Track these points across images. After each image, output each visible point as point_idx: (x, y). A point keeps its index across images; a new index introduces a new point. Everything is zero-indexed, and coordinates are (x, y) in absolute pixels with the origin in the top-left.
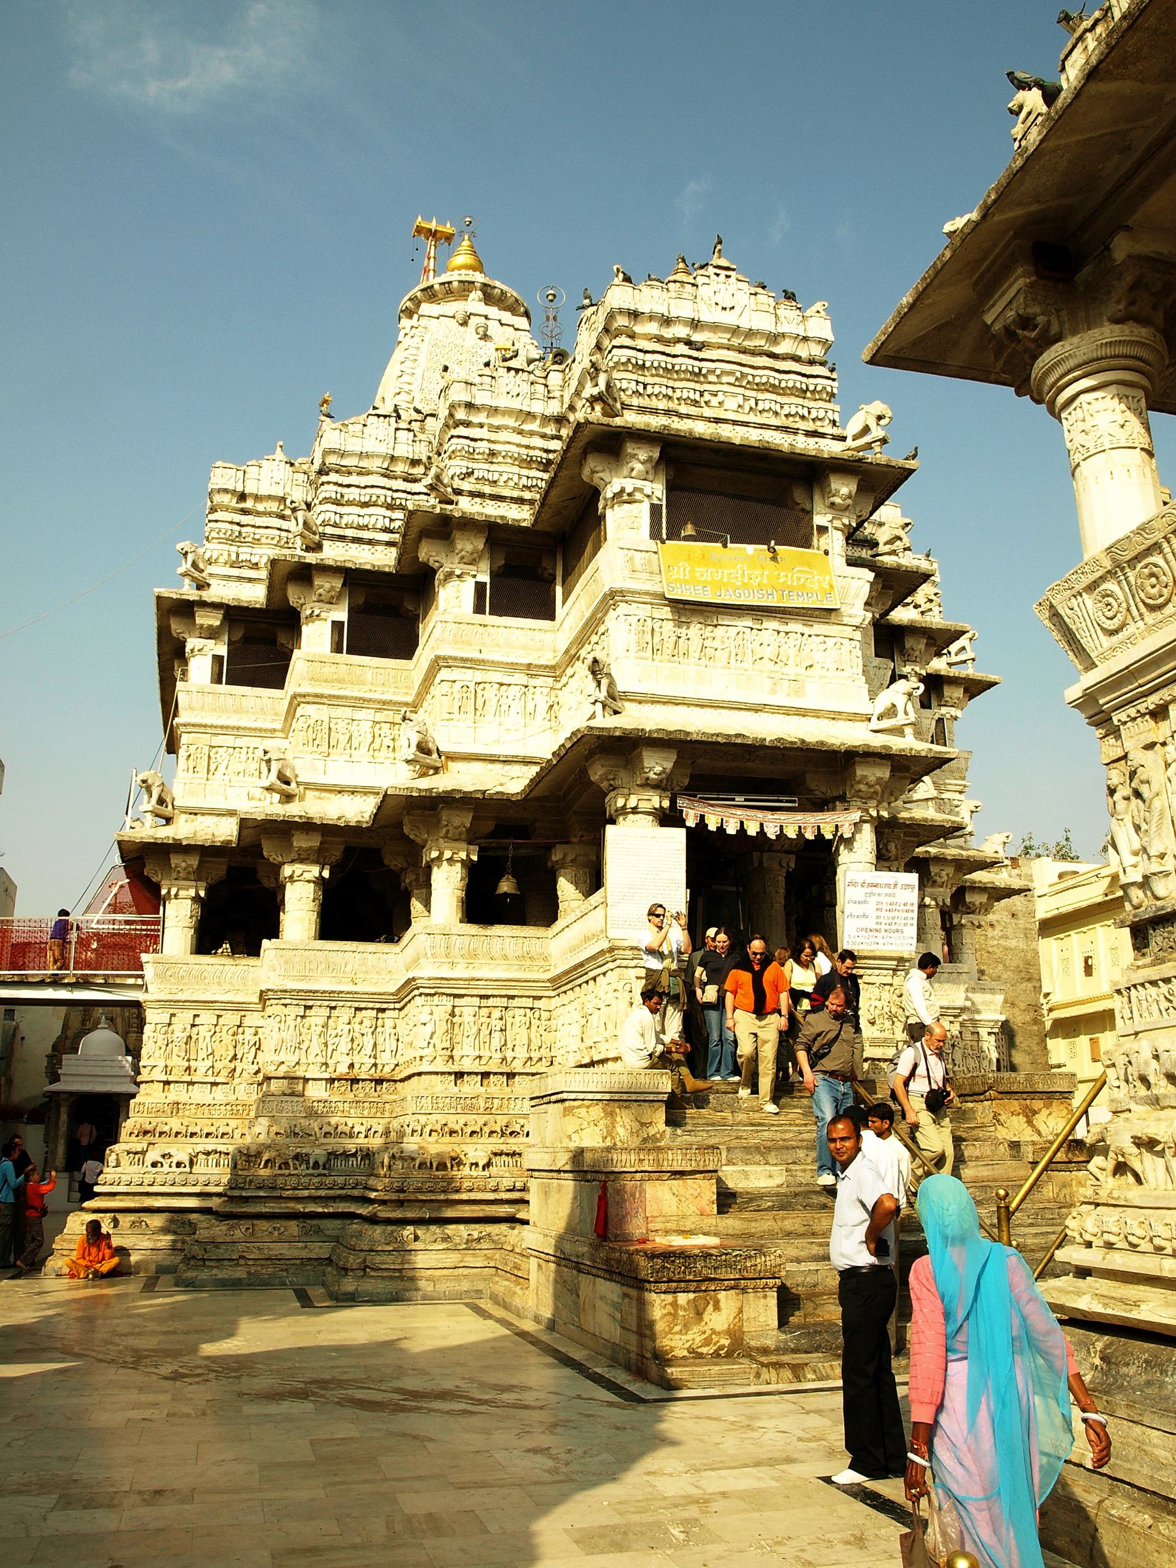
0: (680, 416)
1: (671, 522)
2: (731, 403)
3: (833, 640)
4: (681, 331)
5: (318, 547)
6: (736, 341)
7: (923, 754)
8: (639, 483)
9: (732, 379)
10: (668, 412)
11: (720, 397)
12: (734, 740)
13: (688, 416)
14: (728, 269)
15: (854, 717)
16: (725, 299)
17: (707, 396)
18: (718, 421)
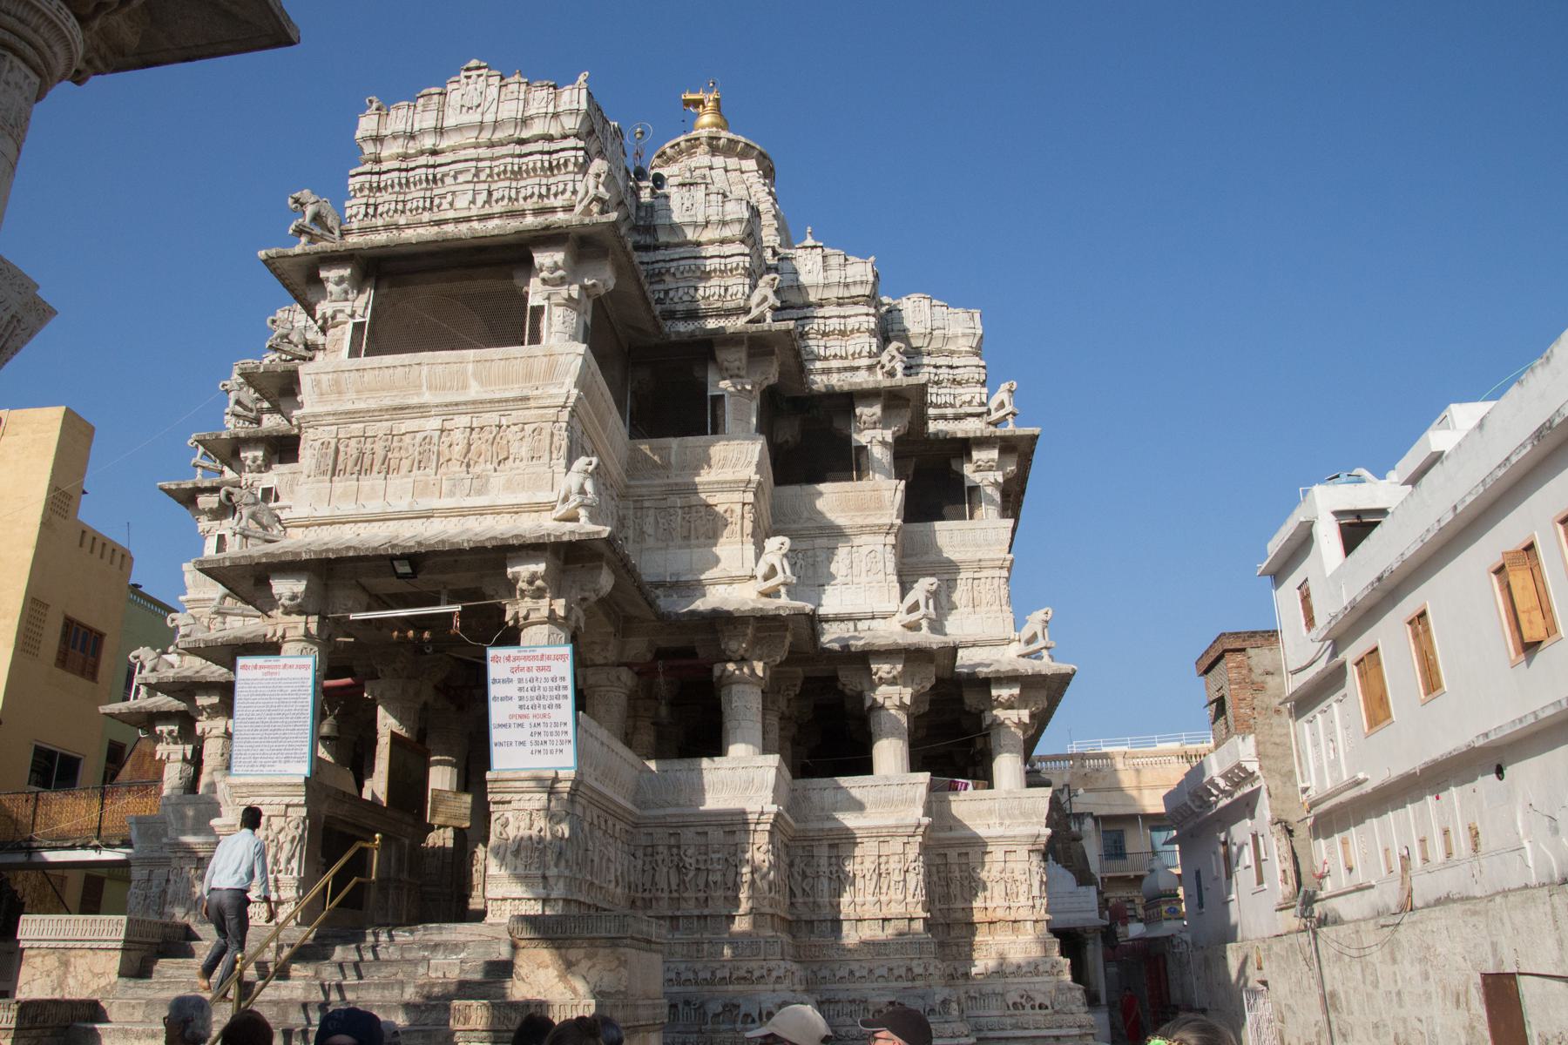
0: (398, 227)
1: (376, 339)
2: (462, 202)
3: (533, 426)
4: (428, 142)
5: (258, 421)
6: (485, 136)
7: (566, 538)
8: (339, 305)
9: (469, 177)
10: (387, 227)
11: (449, 197)
12: (344, 554)
13: (408, 226)
14: (478, 68)
15: (537, 508)
16: (477, 100)
17: (437, 201)
18: (439, 223)
